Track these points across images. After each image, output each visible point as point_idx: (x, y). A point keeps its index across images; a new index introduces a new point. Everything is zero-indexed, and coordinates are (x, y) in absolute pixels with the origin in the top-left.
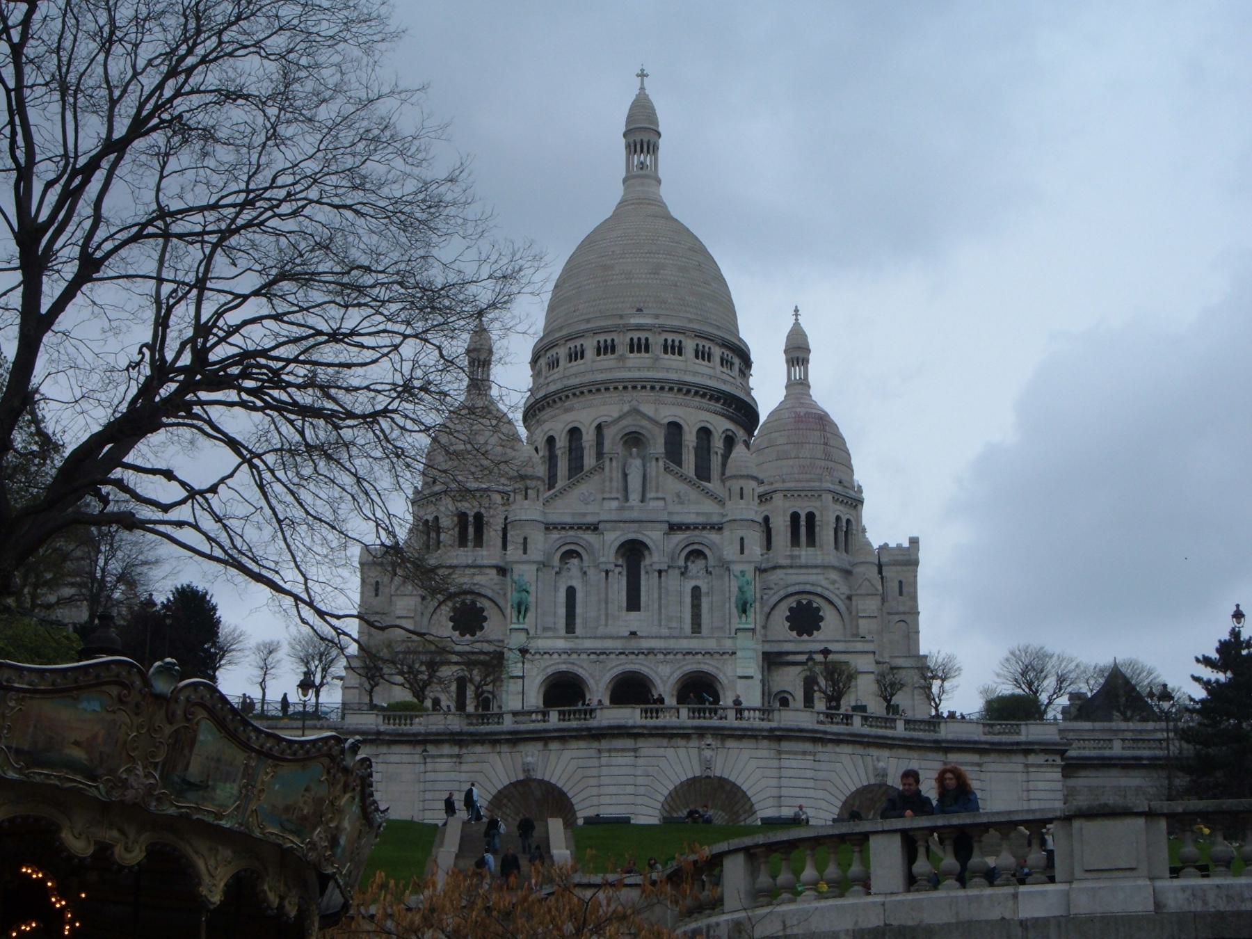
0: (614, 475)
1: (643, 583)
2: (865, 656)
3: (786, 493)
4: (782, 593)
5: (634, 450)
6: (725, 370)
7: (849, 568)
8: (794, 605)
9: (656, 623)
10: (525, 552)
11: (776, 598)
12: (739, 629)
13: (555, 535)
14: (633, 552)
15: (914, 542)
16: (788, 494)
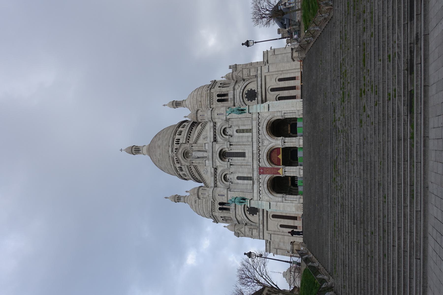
0: (197, 162)
1: (235, 151)
2: (263, 70)
3: (211, 104)
4: (243, 103)
5: (189, 154)
6: (185, 127)
7: (235, 81)
8: (247, 99)
9: (249, 146)
10: (224, 195)
11: (244, 105)
12: (248, 112)
13: (218, 183)
14: (223, 155)
15: (230, 67)
16: (211, 103)
